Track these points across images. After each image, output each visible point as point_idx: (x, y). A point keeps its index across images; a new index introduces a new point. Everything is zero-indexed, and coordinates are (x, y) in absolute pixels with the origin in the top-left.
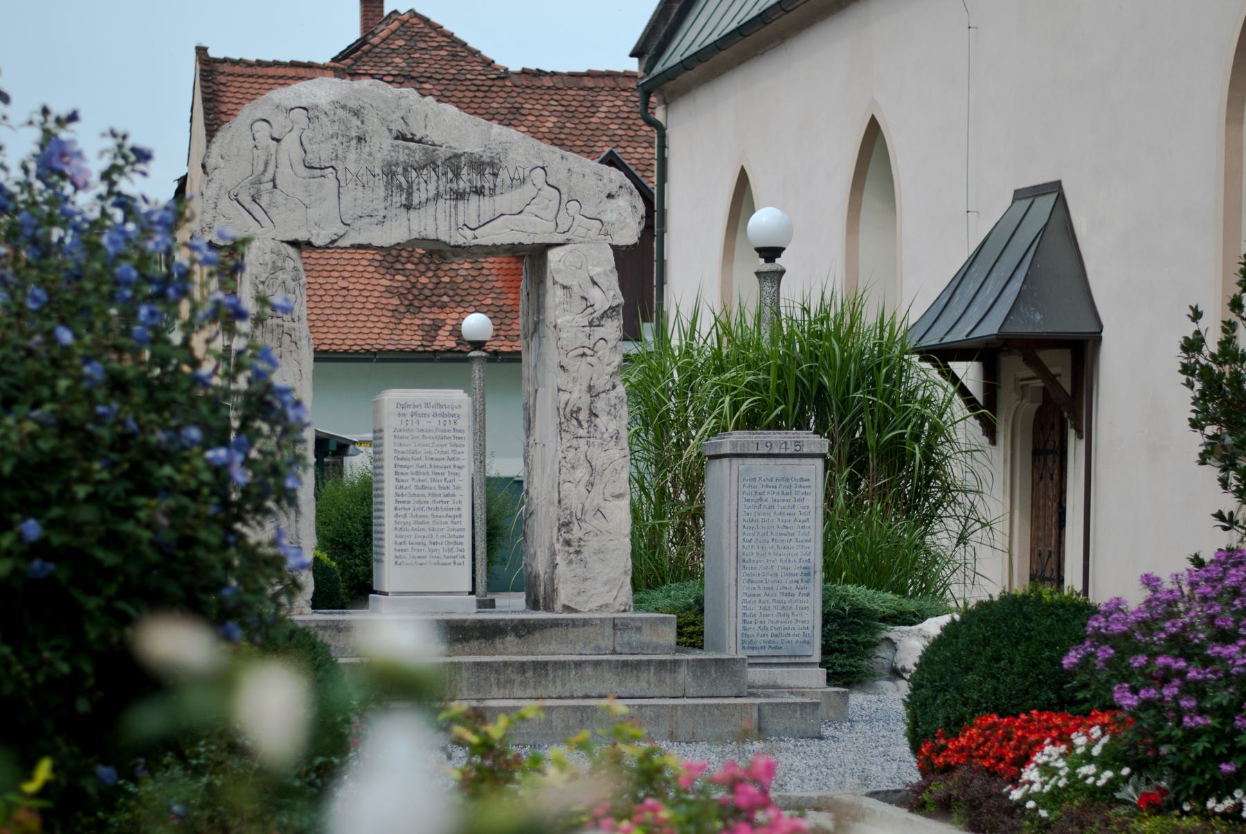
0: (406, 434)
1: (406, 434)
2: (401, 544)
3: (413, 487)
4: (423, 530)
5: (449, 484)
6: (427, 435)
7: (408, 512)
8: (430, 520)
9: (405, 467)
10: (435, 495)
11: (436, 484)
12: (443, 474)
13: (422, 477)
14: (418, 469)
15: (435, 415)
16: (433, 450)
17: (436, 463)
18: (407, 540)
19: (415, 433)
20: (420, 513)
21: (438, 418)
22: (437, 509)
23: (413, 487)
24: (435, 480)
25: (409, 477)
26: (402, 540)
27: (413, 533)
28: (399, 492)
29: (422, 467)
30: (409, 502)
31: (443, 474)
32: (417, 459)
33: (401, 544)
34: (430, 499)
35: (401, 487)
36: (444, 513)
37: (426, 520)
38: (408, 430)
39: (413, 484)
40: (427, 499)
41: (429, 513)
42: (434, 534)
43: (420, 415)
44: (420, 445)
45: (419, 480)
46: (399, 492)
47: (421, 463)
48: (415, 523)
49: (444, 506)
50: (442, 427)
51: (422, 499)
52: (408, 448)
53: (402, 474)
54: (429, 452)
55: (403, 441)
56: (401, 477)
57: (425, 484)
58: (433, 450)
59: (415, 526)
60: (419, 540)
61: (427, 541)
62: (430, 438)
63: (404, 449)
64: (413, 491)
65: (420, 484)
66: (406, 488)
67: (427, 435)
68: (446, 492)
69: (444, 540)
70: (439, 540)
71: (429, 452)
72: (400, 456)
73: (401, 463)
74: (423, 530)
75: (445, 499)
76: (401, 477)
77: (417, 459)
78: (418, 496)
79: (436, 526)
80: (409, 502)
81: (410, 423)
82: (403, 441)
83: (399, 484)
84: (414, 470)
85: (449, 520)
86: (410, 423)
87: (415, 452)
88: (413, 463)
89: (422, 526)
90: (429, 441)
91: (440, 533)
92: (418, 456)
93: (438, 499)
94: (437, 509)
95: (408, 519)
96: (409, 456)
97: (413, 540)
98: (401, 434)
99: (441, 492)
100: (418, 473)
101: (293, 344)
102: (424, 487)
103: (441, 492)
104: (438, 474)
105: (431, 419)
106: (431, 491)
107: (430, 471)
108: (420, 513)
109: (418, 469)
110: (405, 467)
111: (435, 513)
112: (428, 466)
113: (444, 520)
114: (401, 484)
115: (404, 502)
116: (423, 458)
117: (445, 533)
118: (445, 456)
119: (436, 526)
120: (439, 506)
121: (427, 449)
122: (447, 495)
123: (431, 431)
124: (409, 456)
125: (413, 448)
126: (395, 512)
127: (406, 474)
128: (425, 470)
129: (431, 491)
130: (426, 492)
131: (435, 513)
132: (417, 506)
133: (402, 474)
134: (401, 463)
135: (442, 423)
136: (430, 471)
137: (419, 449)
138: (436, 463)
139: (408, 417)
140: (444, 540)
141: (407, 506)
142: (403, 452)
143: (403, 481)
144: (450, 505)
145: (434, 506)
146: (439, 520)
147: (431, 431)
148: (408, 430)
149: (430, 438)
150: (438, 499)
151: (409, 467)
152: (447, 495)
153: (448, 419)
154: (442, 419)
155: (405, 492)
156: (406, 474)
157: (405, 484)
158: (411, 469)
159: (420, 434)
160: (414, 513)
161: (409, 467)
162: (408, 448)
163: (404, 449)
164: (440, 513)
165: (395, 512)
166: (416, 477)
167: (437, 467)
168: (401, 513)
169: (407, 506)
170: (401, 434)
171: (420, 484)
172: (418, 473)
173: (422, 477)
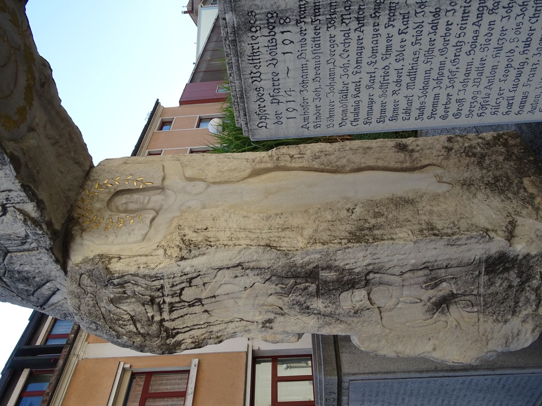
0: (312, 110)
1: (312, 110)
2: (510, 105)
3: (409, 92)
4: (494, 68)
5: (411, 24)
6: (311, 74)
7: (454, 98)
8: (478, 55)
9: (370, 108)
10: (430, 51)
11: (409, 50)
12: (389, 38)
13: (393, 77)
14: (377, 85)
15: (273, 62)
16: (340, 62)
17: (367, 53)
18: (507, 94)
19: (309, 95)
20: (461, 77)
21: (280, 57)
22: (459, 46)
23: (409, 92)
24: (401, 53)
25: (390, 100)
26: (504, 103)
27: (496, 87)
28: (415, 113)
29: (372, 80)
30: (437, 96)
31: (389, 38)
32: (358, 89)
33: (510, 105)
34: (437, 59)
35: (407, 112)
36: (470, 29)
37: (477, 63)
38: (305, 105)
39: (404, 91)
40: (436, 65)
41: (464, 59)
42: (508, 47)
43: (276, 88)
44: (331, 86)
45: (398, 82)
46: (415, 113)
47: (366, 80)
48: (476, 83)
49: (455, 30)
50: (294, 48)
51: (434, 74)
52: (337, 104)
53: (383, 111)
54: (345, 67)
55: (325, 114)
56: (389, 113)
57: (405, 72)
58: (340, 62)
59: (484, 82)
60: (513, 73)
61: (518, 59)
62: (317, 68)
63: (338, 111)
64: (417, 92)
65: (405, 79)
66: (410, 103)
67: (311, 74)
68: (427, 28)
69: (526, 26)
70: (523, 37)
71: (345, 67)
72: (351, 117)
73: (363, 114)
74: (494, 68)
75: (442, 29)
76: (389, 113)
77: (358, 89)
78: (426, 82)
79: (494, 43)
80: (437, 96)
81: (291, 105)
82: (325, 114)
83: (401, 116)
84: (377, 92)
85: (487, 18)
86: (291, 105)
87: (344, 93)
88: (364, 96)
89: (487, 71)
90: (325, 71)
91: (511, 34)
92: (352, 87)
93: (439, 44)
94: (459, 46)
95: (468, 96)
96: (351, 101)
97: (508, 85)
98: (312, 118)
99: (425, 39)
100: (384, 85)
101: (194, 282)
102: (413, 73)
103: (425, 39)
104: (388, 48)
105: (281, 68)
106: (422, 58)
107: (381, 64)
108: (461, 77)
109: (377, 85)
110: (370, 108)
111: (466, 48)
112: (371, 69)
113: (484, 29)
114: (401, 111)
115: (435, 105)
116: (356, 78)
117: (511, 24)
118: (354, 35)
119: (494, 43)
120: (453, 40)
121: (339, 71)
122: (435, 26)
123: (304, 68)
124: (351, 101)
125: (336, 97)
126: (451, 117)
127: (383, 104)
128: (380, 72)
129: (422, 58)
130: (422, 67)
131: (466, 48)
132: (446, 82)
133: (383, 111)
134: (363, 114)
135: (287, 49)
136: (381, 64)
137: (339, 86)
138: (367, 53)
139: (282, 107)
140: (526, 26)
141: (443, 99)
142: (344, 112)
143: (395, 109)
144: (457, 19)
145: (451, 51)
146: (481, 40)
147: (304, 68)
148: (305, 105)
149: (317, 68)
150: (439, 44)
151: (372, 101)
152: (435, 26)
153: (279, 37)
154: (281, 48)
155: (416, 104)
156: (383, 104)
157: (403, 104)
158: (376, 98)
159: (312, 86)
160: (458, 86)
161: (372, 101)
162: (337, 104)
163: (338, 111)
164: (468, 38)
165: (451, 117)
166: (392, 87)
167: (374, 52)
168: (453, 108)
169: (443, 99)
170: (312, 118)
171: (405, 79)
172: (384, 85)
173: (393, 77)
